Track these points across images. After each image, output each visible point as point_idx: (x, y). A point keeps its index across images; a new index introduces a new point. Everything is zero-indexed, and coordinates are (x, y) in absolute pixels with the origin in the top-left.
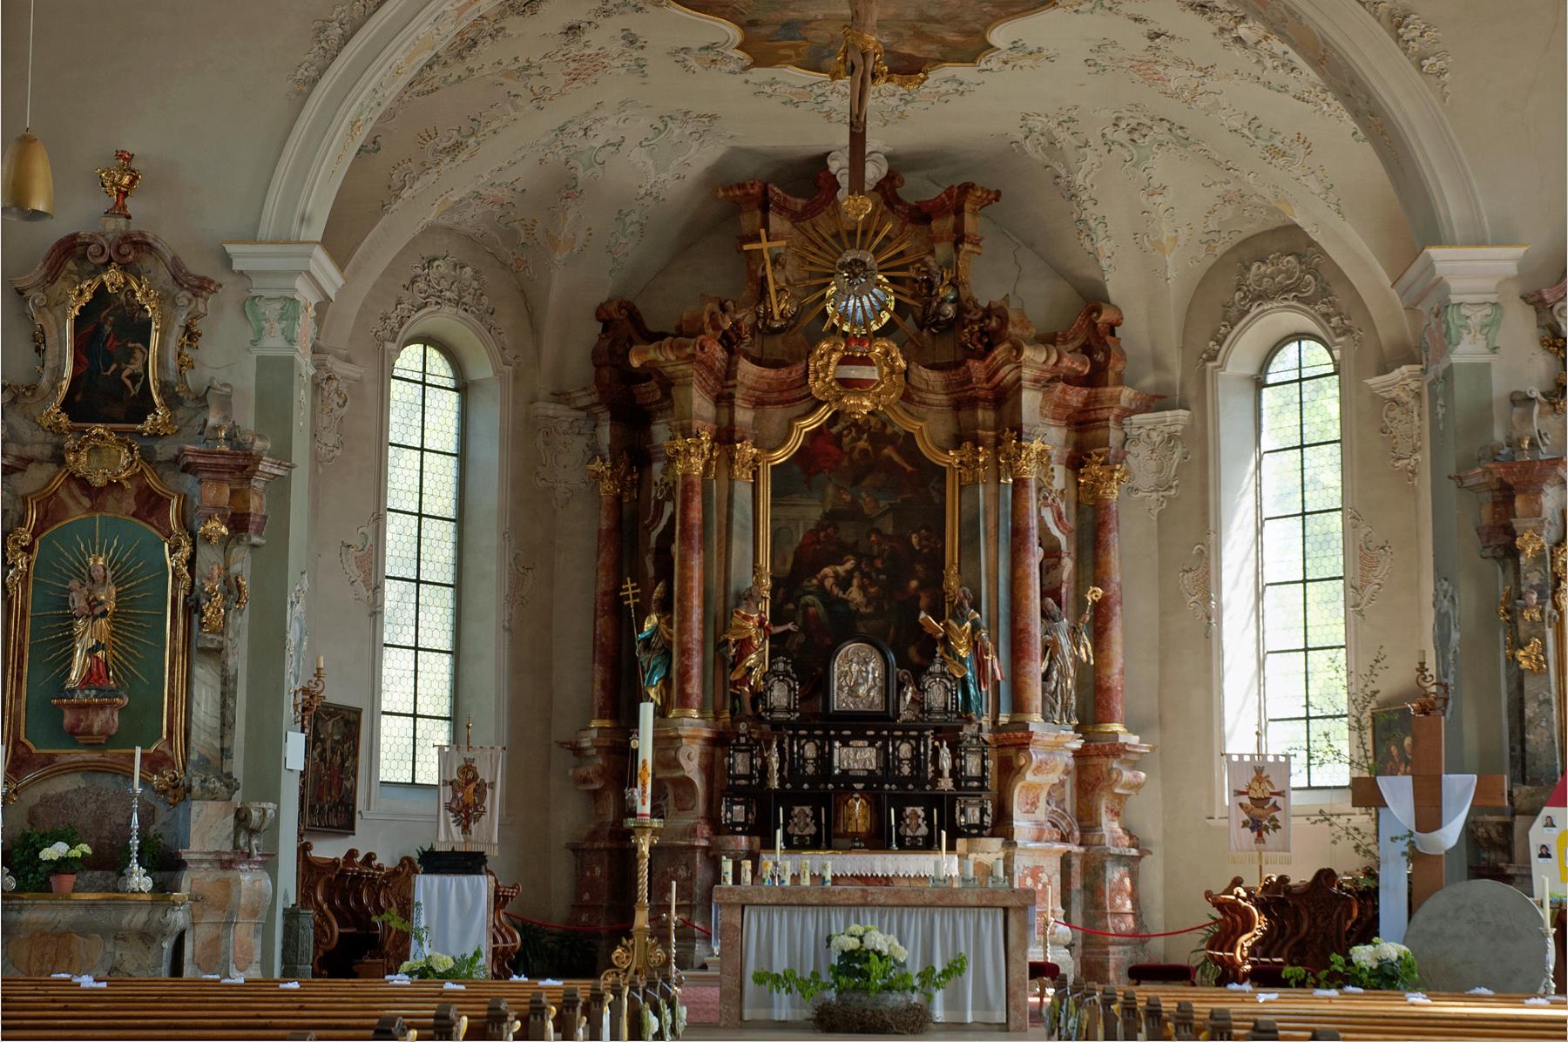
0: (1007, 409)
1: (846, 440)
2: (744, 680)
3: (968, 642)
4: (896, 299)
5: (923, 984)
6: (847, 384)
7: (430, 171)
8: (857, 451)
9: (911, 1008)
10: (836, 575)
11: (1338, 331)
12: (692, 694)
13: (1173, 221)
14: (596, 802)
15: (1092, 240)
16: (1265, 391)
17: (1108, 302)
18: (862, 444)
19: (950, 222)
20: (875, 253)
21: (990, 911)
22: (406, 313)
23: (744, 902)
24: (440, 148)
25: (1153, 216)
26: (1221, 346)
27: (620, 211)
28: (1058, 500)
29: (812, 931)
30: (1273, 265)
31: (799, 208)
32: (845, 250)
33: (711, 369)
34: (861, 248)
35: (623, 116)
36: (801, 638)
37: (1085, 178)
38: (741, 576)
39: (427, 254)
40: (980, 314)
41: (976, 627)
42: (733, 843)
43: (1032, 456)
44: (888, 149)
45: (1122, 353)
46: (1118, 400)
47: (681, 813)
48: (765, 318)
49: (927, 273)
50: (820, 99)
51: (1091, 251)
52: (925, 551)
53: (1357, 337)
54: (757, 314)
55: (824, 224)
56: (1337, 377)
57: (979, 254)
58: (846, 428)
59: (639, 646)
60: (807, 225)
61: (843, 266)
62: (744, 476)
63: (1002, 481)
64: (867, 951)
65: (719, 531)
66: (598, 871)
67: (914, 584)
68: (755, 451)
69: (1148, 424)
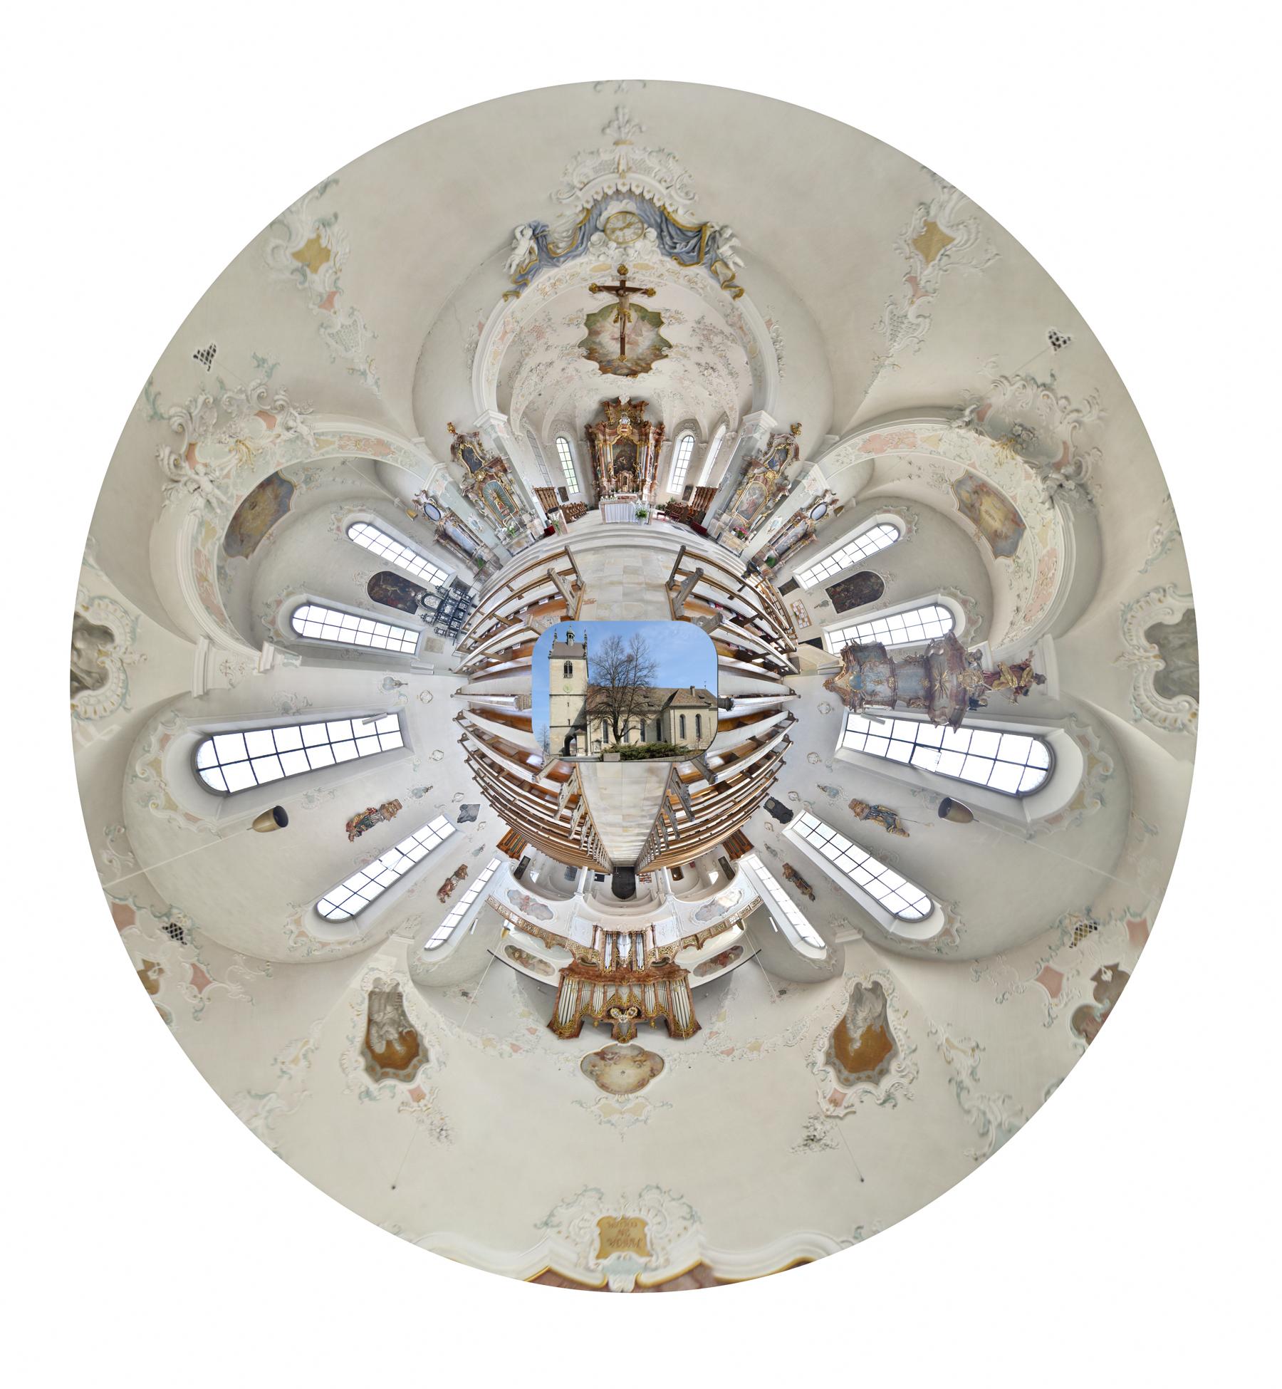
38: (609, 460)
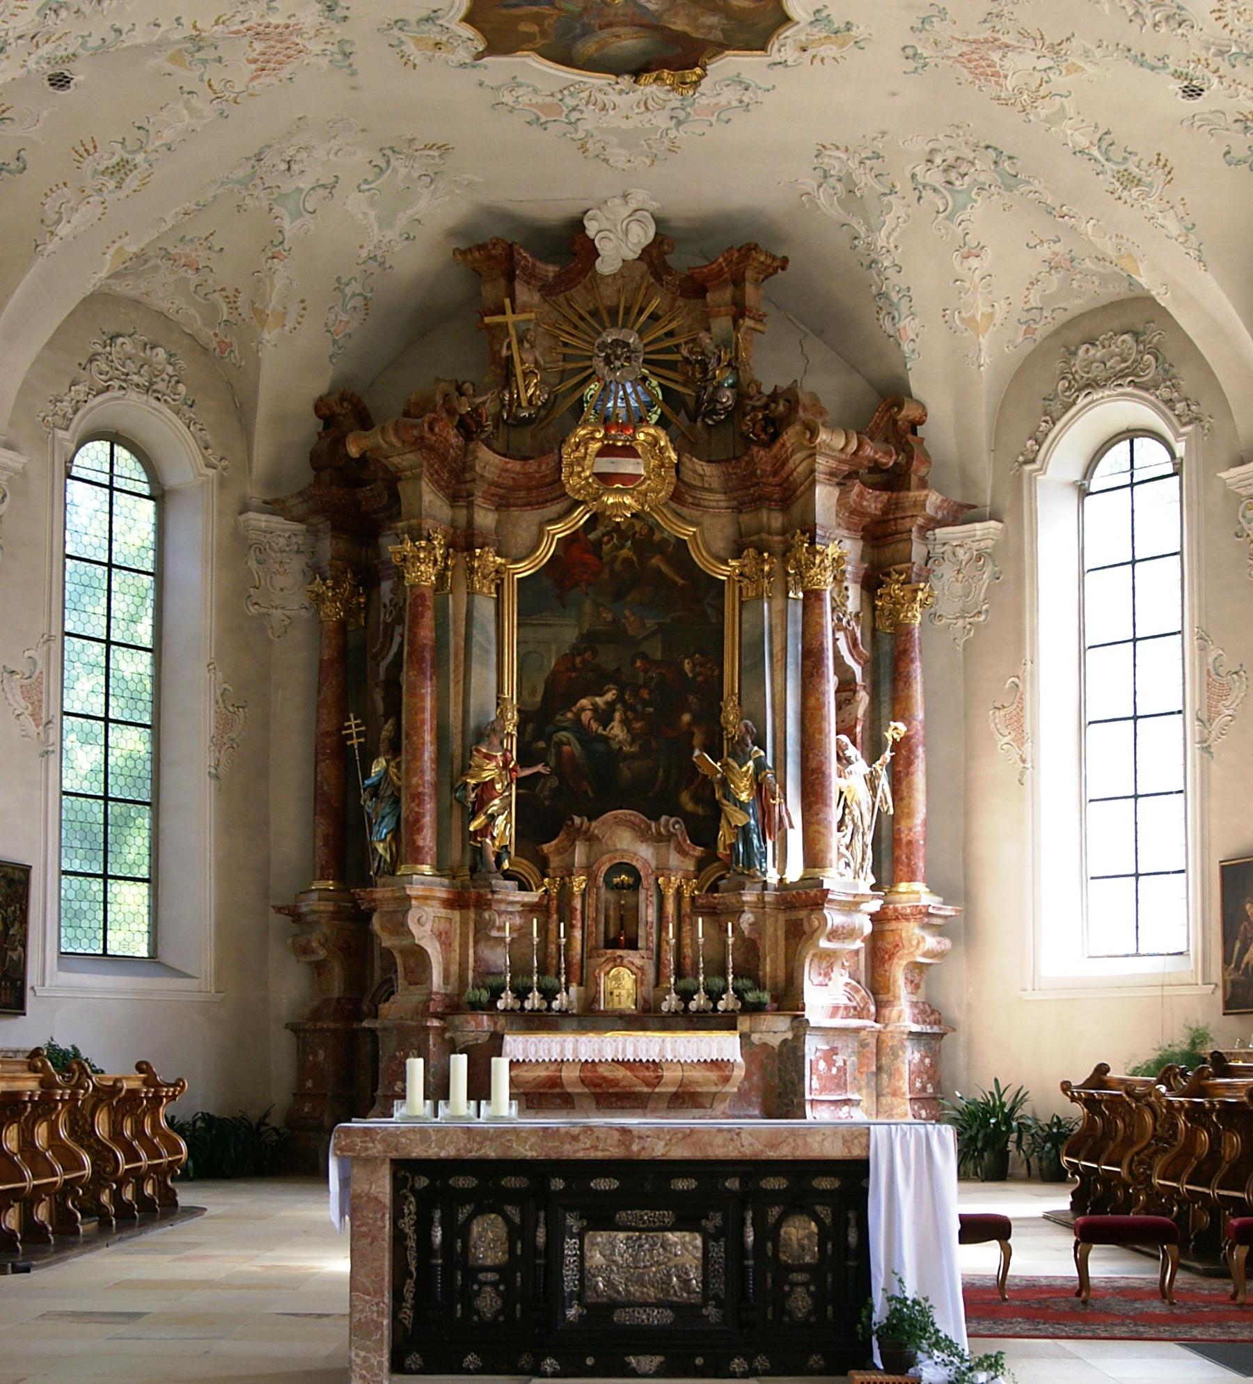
0: (796, 510)
1: (606, 548)
2: (485, 830)
3: (751, 785)
4: (662, 414)
6: (605, 479)
7: (91, 199)
8: (618, 562)
10: (595, 708)
11: (1184, 420)
12: (423, 847)
13: (990, 292)
14: (319, 975)
15: (893, 318)
16: (1088, 499)
17: (911, 396)
18: (625, 552)
19: (727, 294)
20: (641, 333)
22: (82, 397)
24: (101, 168)
25: (967, 285)
26: (1040, 445)
27: (339, 279)
28: (853, 623)
30: (1104, 347)
31: (551, 274)
32: (605, 328)
33: (443, 459)
34: (623, 327)
35: (334, 144)
36: (554, 782)
37: (888, 238)
39: (111, 329)
40: (764, 400)
41: (760, 766)
42: (473, 1023)
43: (827, 563)
44: (656, 205)
45: (926, 455)
46: (924, 507)
47: (412, 987)
48: (510, 405)
49: (703, 353)
50: (574, 116)
51: (892, 333)
52: (700, 679)
53: (1207, 426)
54: (502, 400)
55: (580, 298)
56: (1177, 478)
57: (762, 333)
58: (608, 533)
59: (365, 795)
60: (561, 298)
61: (604, 346)
62: (485, 590)
63: (791, 595)
65: (456, 655)
66: (321, 1055)
67: (686, 718)
68: (499, 560)
69: (954, 539)
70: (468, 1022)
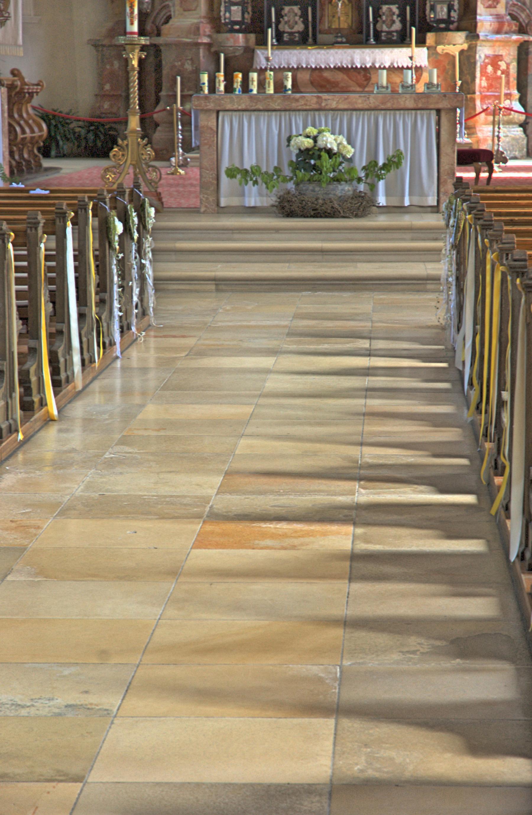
5: (367, 176)
9: (358, 196)
21: (425, 112)
23: (219, 108)
29: (276, 132)
42: (232, 40)
47: (186, 13)
64: (320, 150)
70: (228, 39)
